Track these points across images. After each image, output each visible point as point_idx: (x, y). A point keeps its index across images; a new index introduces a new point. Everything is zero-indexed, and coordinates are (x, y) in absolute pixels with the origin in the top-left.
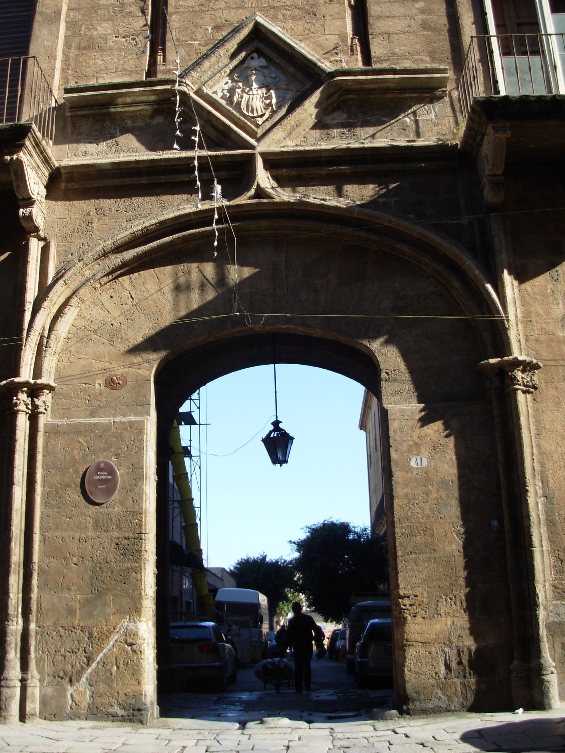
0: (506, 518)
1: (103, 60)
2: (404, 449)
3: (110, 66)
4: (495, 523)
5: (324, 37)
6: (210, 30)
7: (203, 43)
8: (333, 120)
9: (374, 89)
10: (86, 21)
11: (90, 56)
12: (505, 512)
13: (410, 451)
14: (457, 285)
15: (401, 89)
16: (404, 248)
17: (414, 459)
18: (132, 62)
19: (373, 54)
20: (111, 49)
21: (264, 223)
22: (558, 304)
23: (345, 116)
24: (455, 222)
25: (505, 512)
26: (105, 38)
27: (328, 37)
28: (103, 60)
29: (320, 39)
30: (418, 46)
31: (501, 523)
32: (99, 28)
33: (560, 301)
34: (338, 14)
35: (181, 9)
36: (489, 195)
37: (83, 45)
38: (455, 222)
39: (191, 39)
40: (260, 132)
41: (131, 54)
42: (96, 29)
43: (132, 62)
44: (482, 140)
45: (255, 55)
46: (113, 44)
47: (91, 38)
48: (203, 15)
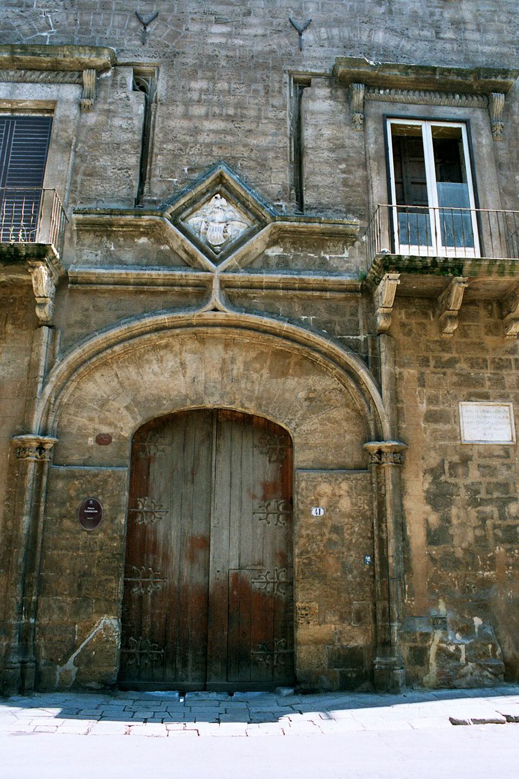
0: (376, 555)
1: (103, 187)
2: (308, 502)
3: (108, 192)
4: (368, 558)
5: (270, 186)
6: (186, 171)
7: (180, 181)
8: (272, 252)
9: (303, 232)
10: (90, 152)
11: (93, 182)
12: (376, 551)
13: (312, 503)
14: (353, 386)
15: (323, 233)
16: (317, 355)
17: (314, 510)
18: (125, 191)
19: (305, 203)
20: (109, 179)
21: (218, 330)
22: (422, 403)
23: (282, 249)
24: (355, 337)
25: (376, 551)
26: (105, 168)
27: (274, 186)
28: (103, 187)
29: (267, 187)
30: (339, 199)
31: (373, 559)
32: (101, 160)
33: (425, 401)
34: (282, 168)
35: (165, 152)
36: (382, 322)
37: (87, 172)
38: (355, 337)
39: (171, 177)
40: (218, 256)
41: (124, 184)
42: (99, 161)
43: (125, 191)
44: (379, 282)
45: (218, 196)
46: (111, 175)
47: (94, 167)
48: (181, 158)
